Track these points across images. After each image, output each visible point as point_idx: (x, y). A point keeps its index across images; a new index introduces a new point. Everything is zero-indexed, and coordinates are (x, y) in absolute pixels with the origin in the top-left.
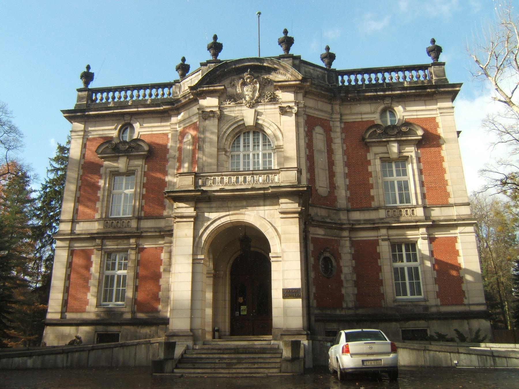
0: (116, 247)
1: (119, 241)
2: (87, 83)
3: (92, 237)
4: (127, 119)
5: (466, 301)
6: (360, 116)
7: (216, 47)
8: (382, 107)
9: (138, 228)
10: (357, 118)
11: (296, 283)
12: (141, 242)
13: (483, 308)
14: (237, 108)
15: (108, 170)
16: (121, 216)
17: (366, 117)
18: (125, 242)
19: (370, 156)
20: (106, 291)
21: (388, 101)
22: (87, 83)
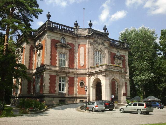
0: (62, 75)
1: (64, 74)
2: (49, 18)
3: (57, 72)
4: (64, 36)
5: (127, 96)
6: (113, 52)
7: (91, 25)
8: (117, 50)
9: (68, 71)
10: (113, 52)
11: (125, 92)
12: (69, 75)
13: (130, 97)
14: (96, 44)
15: (59, 51)
16: (62, 66)
17: (115, 52)
18: (65, 74)
19: (115, 62)
20: (59, 88)
21: (118, 49)
22: (49, 18)
